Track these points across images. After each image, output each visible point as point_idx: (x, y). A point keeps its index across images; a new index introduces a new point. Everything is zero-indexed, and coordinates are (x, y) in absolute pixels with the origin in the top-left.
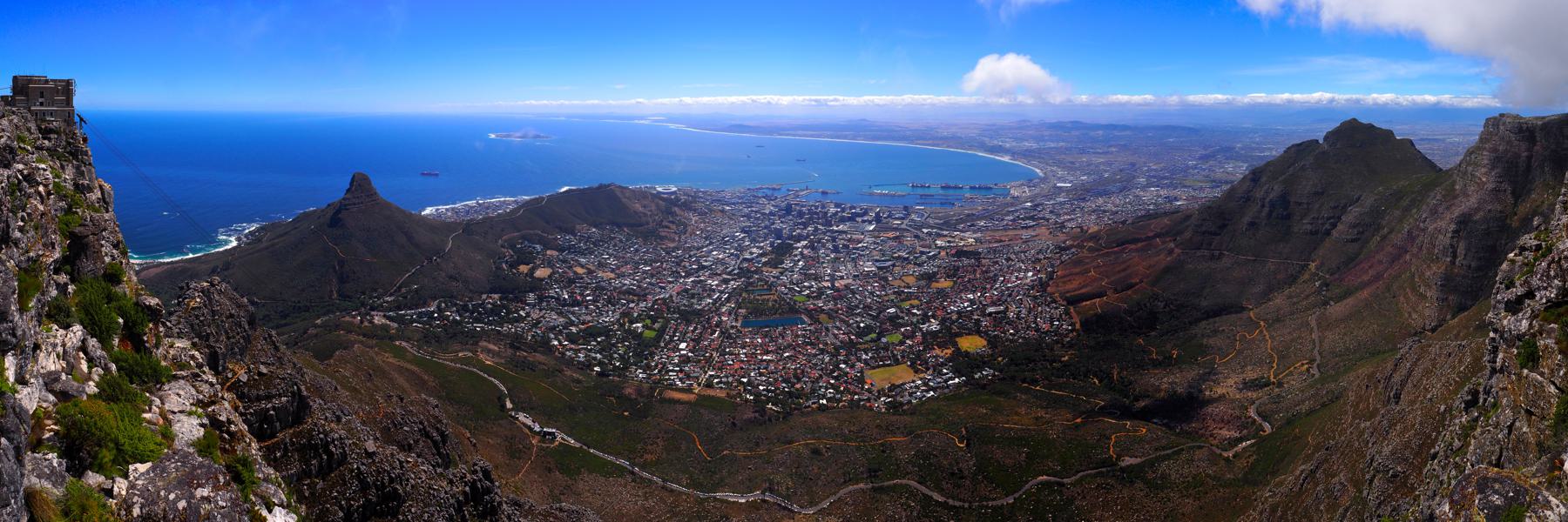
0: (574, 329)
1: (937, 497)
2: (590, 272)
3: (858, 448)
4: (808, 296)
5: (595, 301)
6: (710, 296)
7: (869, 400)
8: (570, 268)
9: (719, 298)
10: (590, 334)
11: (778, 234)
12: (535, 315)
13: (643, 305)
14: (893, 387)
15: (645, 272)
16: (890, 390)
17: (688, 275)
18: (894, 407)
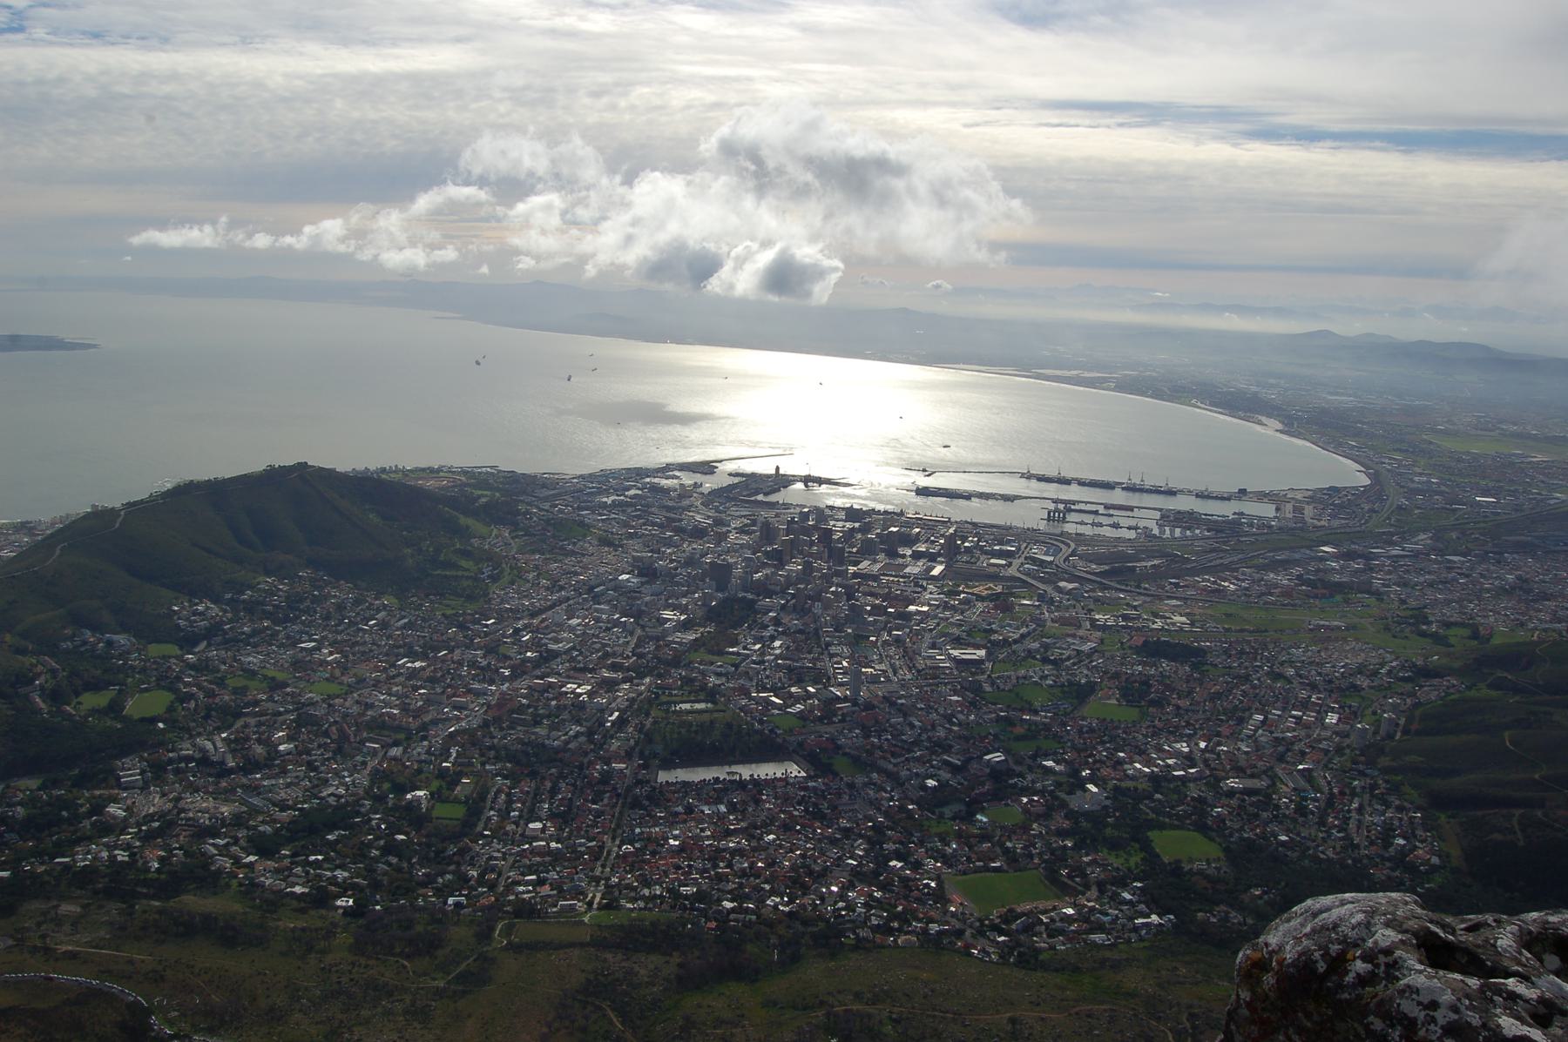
2: (275, 686)
10: (307, 830)
11: (720, 573)
15: (414, 673)
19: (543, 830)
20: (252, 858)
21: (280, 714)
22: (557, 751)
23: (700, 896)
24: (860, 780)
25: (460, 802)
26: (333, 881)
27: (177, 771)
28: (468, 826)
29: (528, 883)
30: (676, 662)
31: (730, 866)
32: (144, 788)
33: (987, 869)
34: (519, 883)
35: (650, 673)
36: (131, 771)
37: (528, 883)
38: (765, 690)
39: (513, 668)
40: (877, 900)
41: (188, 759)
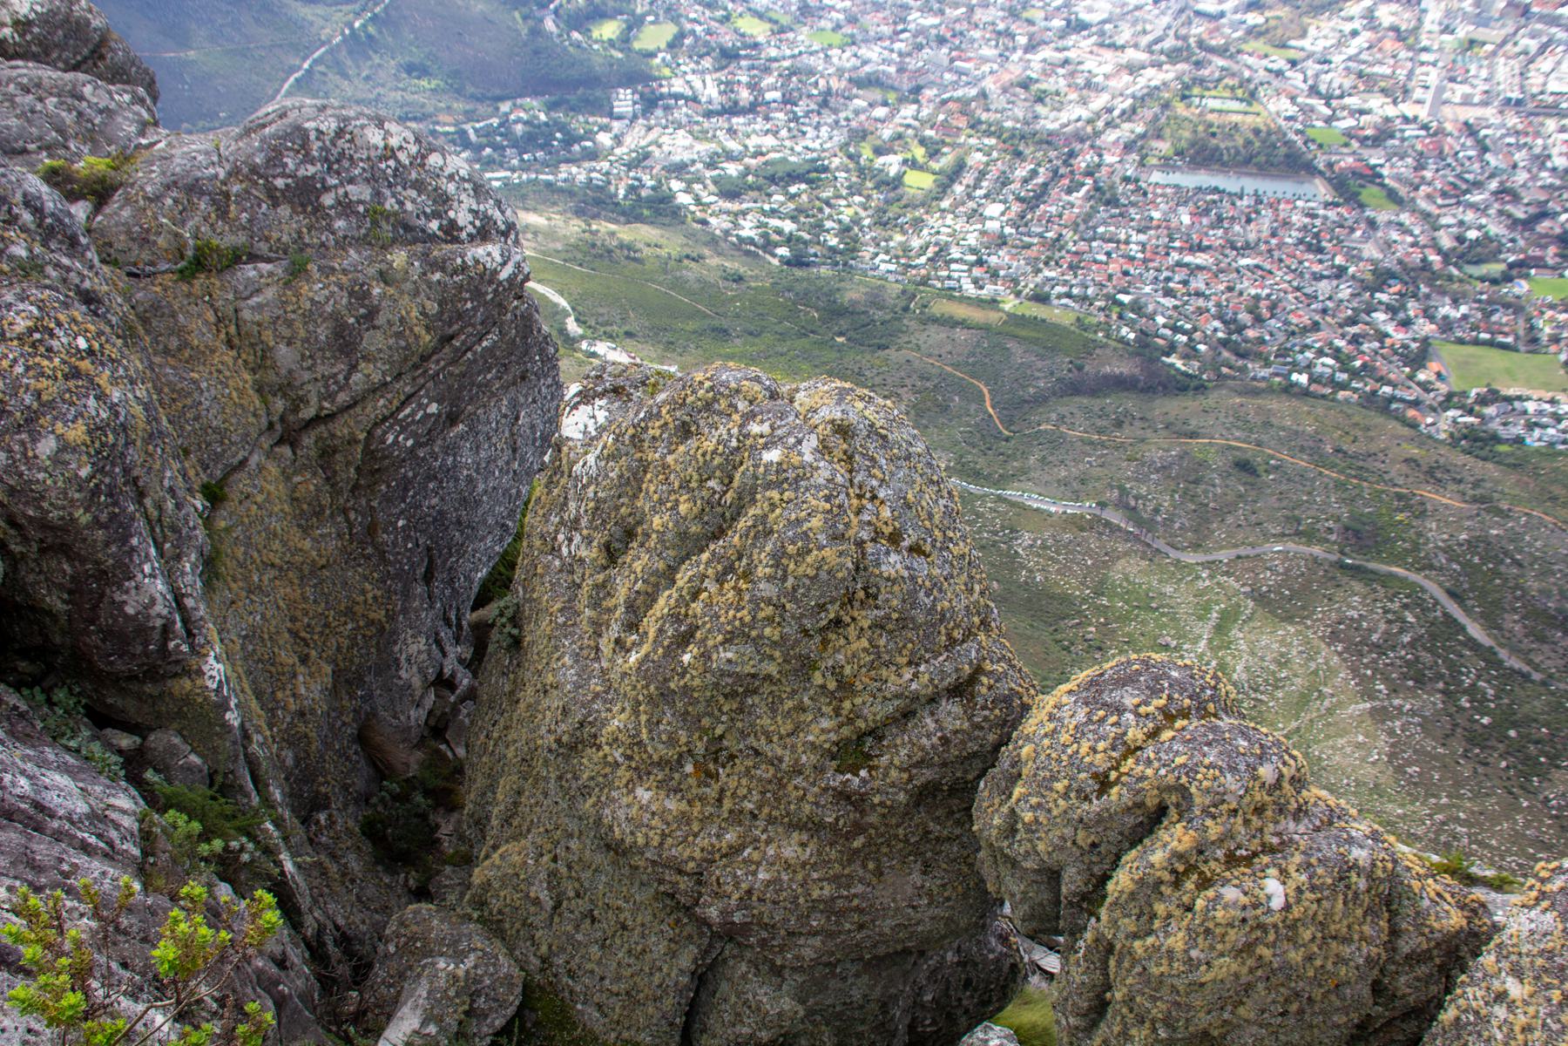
0: (732, 169)
1: (1475, 630)
3: (1339, 486)
4: (1349, 134)
5: (788, 101)
6: (1084, 102)
7: (1416, 404)
8: (727, 18)
9: (1110, 110)
12: (636, 138)
13: (908, 111)
14: (1491, 397)
15: (922, 31)
16: (1483, 401)
17: (1031, 47)
18: (1478, 441)
19: (1003, 214)
20: (713, 198)
21: (776, 60)
22: (1050, 134)
23: (1137, 307)
24: (1382, 218)
25: (934, 173)
26: (779, 232)
27: (667, 108)
28: (930, 201)
29: (965, 263)
30: (1222, 51)
31: (1185, 283)
32: (635, 117)
33: (1491, 344)
34: (956, 261)
35: (1186, 60)
36: (624, 100)
37: (965, 263)
38: (1318, 94)
39: (1031, 37)
40: (1338, 350)
41: (677, 97)
